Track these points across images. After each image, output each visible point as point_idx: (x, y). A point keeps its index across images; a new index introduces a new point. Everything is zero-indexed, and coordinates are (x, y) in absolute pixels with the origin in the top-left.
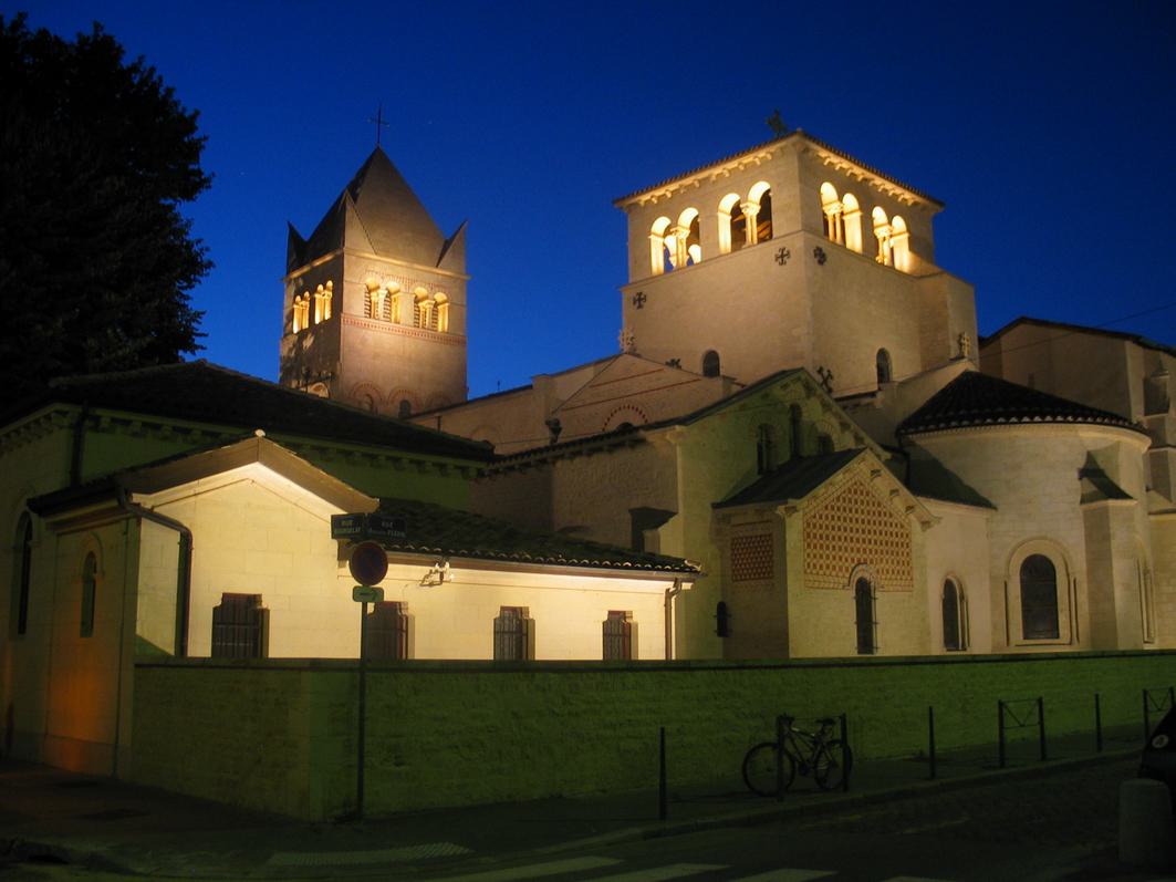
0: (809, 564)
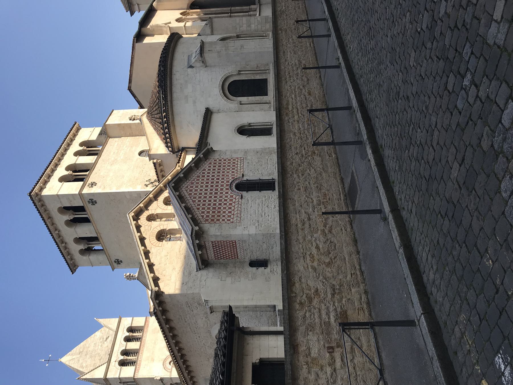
0: (229, 220)
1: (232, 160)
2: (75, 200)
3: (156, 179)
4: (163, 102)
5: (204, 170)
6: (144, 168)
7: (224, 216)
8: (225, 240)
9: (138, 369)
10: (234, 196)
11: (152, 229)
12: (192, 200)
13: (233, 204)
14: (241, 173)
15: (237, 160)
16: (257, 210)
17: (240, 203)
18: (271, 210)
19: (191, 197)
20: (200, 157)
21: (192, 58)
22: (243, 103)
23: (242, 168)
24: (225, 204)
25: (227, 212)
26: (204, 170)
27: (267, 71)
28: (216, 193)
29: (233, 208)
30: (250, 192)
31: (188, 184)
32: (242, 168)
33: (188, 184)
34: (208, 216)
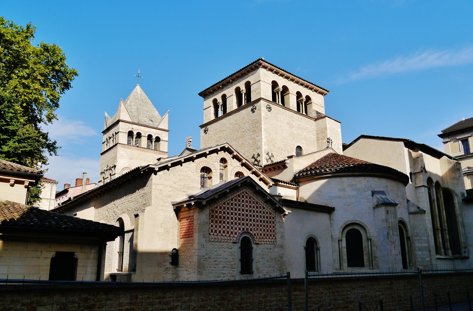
0: (212, 231)
1: (274, 233)
2: (256, 94)
3: (274, 162)
4: (338, 169)
5: (264, 208)
6: (284, 151)
7: (216, 227)
8: (194, 227)
9: (124, 146)
10: (236, 236)
11: (213, 163)
12: (234, 198)
13: (228, 235)
14: (260, 243)
15: (274, 238)
16: (221, 257)
17: (229, 241)
18: (221, 270)
19: (236, 196)
20: (276, 204)
21: (381, 195)
22: (340, 243)
23: (265, 243)
24: (228, 228)
25: (220, 229)
26: (264, 208)
27: (371, 267)
28: (239, 219)
29: (224, 234)
30: (239, 250)
31: (250, 194)
32: (265, 243)
33: (250, 194)
34: (217, 212)
